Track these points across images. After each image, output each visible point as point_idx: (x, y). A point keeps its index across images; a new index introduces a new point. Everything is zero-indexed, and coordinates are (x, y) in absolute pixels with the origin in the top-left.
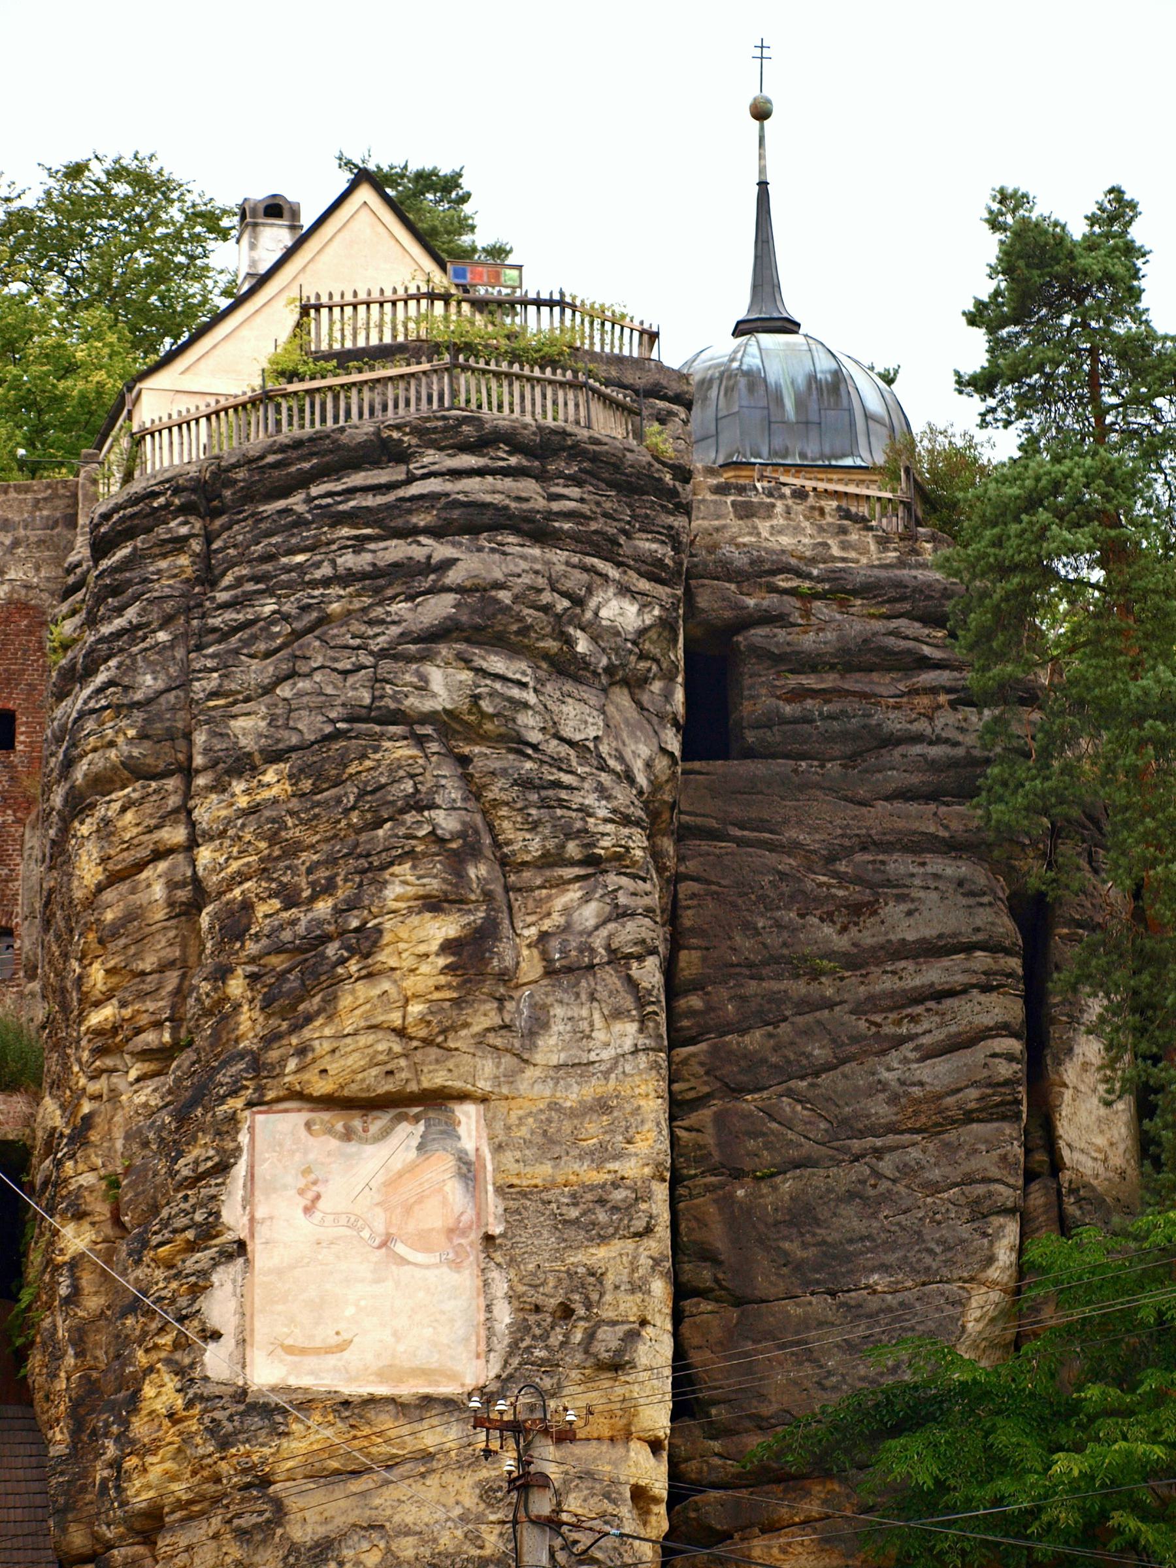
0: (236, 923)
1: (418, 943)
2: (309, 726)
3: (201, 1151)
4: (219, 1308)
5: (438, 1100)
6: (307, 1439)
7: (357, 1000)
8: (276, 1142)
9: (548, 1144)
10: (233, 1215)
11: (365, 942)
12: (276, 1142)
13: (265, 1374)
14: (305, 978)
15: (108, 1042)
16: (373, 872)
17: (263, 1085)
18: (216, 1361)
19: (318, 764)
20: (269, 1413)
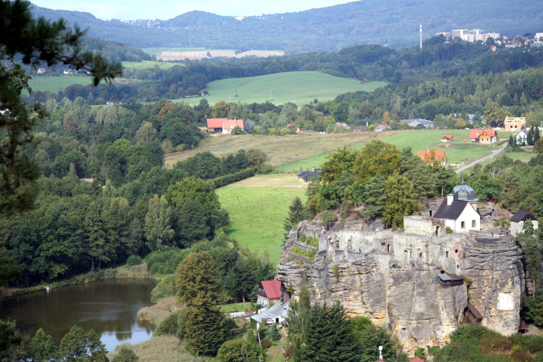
0: (497, 281)
1: (510, 283)
2: (503, 269)
3: (495, 295)
4: (498, 305)
5: (510, 292)
6: (504, 313)
7: (507, 287)
8: (501, 295)
9: (516, 294)
10: (498, 299)
11: (507, 283)
12: (501, 295)
13: (501, 309)
14: (503, 285)
15: (486, 286)
16: (508, 279)
17: (500, 290)
18: (498, 308)
19: (503, 272)
20: (502, 311)
